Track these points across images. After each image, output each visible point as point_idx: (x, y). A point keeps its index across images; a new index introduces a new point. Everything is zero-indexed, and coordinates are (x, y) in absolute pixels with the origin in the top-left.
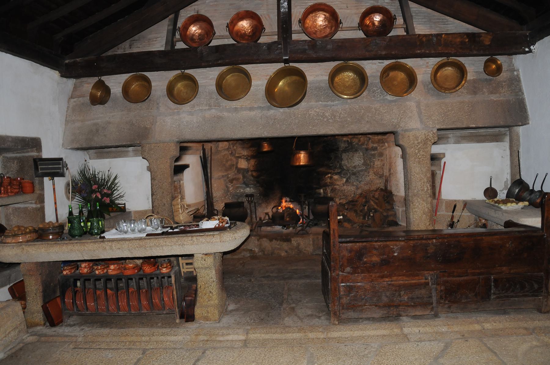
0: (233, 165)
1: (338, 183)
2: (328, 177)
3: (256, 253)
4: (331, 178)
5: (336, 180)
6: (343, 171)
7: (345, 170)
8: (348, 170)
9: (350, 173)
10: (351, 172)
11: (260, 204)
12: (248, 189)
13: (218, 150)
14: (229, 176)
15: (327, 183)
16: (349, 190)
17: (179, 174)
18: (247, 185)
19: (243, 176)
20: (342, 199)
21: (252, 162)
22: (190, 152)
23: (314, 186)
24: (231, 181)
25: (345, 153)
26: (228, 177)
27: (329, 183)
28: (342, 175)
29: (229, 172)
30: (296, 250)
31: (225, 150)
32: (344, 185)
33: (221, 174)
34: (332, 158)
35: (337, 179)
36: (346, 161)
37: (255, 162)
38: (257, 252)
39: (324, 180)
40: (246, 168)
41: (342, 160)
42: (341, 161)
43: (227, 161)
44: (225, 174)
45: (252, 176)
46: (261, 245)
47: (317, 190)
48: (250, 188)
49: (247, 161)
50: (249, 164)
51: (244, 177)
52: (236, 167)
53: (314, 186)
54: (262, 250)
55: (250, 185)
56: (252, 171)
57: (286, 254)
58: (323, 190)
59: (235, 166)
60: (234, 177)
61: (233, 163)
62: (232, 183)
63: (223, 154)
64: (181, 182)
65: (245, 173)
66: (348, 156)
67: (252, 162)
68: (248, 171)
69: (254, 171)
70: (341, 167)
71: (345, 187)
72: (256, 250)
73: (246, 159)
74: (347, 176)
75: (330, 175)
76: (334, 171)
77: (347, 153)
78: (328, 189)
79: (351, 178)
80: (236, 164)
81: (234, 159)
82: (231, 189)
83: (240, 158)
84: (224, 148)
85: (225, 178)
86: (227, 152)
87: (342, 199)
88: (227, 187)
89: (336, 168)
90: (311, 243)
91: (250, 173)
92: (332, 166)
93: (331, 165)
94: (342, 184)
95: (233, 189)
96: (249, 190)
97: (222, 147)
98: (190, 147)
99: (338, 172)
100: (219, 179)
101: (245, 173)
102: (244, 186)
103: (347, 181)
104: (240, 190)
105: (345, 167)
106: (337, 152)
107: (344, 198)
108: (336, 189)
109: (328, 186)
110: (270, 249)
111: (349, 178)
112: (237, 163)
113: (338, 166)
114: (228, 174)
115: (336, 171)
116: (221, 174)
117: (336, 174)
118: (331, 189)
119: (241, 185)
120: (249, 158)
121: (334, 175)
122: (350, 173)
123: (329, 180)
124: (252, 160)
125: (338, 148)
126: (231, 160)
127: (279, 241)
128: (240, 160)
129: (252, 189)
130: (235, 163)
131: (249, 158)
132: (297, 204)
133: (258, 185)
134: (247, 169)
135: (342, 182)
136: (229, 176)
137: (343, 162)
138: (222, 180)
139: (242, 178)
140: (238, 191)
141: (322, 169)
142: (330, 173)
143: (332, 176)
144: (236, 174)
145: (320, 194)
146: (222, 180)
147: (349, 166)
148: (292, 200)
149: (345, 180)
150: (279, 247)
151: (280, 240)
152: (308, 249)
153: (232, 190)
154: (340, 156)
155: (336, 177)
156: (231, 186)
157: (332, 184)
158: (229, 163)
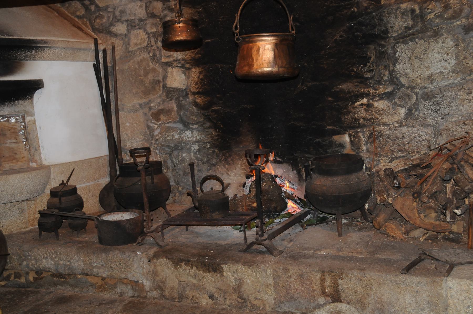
0: (159, 82)
1: (385, 119)
2: (362, 105)
3: (147, 292)
4: (369, 106)
5: (381, 112)
6: (399, 89)
7: (402, 86)
8: (412, 88)
9: (417, 94)
10: (420, 93)
11: (214, 165)
12: (188, 133)
13: (129, 52)
14: (152, 105)
15: (356, 120)
16: (415, 137)
17: (21, 102)
18: (186, 125)
19: (177, 106)
20: (397, 158)
21: (195, 73)
22: (51, 53)
23: (328, 127)
24: (156, 116)
25: (405, 43)
26: (150, 108)
27: (364, 119)
28: (397, 100)
29: (151, 97)
30: (235, 296)
31: (141, 49)
32: (401, 126)
33: (136, 101)
34: (370, 58)
35: (383, 110)
36: (408, 65)
37: (200, 73)
38: (147, 288)
39: (350, 112)
40: (183, 87)
41: (396, 61)
42: (394, 65)
43: (146, 74)
44: (145, 100)
45: (196, 104)
46: (155, 273)
47: (336, 138)
48: (192, 130)
49: (184, 72)
50: (188, 78)
51: (180, 107)
52: (164, 87)
53: (328, 127)
54: (160, 287)
55: (193, 124)
56: (194, 94)
57: (210, 301)
58: (350, 136)
59: (161, 84)
60: (160, 108)
61: (157, 78)
62: (158, 120)
63: (139, 59)
64: (28, 118)
65: (181, 99)
66: (413, 50)
67: (195, 73)
68: (187, 94)
69: (198, 93)
70: (394, 80)
71: (404, 129)
72: (147, 284)
73: (180, 67)
74: (409, 104)
75: (365, 101)
76: (376, 90)
77: (410, 44)
78: (360, 134)
79: (421, 107)
80: (163, 79)
81: (160, 70)
82: (156, 133)
83: (170, 66)
84: (139, 47)
85: (146, 110)
86: (146, 55)
87: (397, 158)
88: (149, 127)
89: (379, 82)
90: (271, 281)
91: (191, 98)
92: (372, 78)
93: (368, 75)
94: (397, 122)
95: (159, 133)
96: (190, 136)
97: (136, 44)
98: (45, 42)
99: (385, 93)
100: (135, 111)
101: (181, 99)
102: (180, 126)
103: (409, 114)
104: (173, 136)
105: (403, 80)
106: (383, 43)
107: (400, 157)
108: (380, 134)
109: (361, 126)
110: (176, 284)
111: (416, 106)
112: (165, 77)
113: (385, 78)
114: (150, 101)
115: (381, 90)
116: (136, 101)
117: (381, 97)
118: (368, 133)
119: (174, 125)
120: (187, 66)
121: (377, 101)
122: (417, 94)
123: (362, 113)
124: (193, 70)
125: (386, 32)
126: (154, 70)
127: (195, 268)
128: (170, 69)
129: (196, 134)
130: (160, 78)
131: (187, 66)
132: (290, 168)
133: (208, 124)
134: (185, 89)
135: (396, 118)
136: (152, 105)
137: (398, 68)
138: (140, 113)
139: (175, 108)
140: (170, 138)
141: (346, 86)
142: (367, 95)
143: (371, 102)
144: (164, 101)
145: (342, 146)
146: (140, 113)
147: (413, 75)
148: (278, 159)
149: (403, 112)
150: (195, 282)
151: (197, 267)
152: (264, 296)
153: (158, 135)
154: (390, 51)
155: (380, 105)
156: (156, 126)
157: (371, 121)
158: (151, 77)
